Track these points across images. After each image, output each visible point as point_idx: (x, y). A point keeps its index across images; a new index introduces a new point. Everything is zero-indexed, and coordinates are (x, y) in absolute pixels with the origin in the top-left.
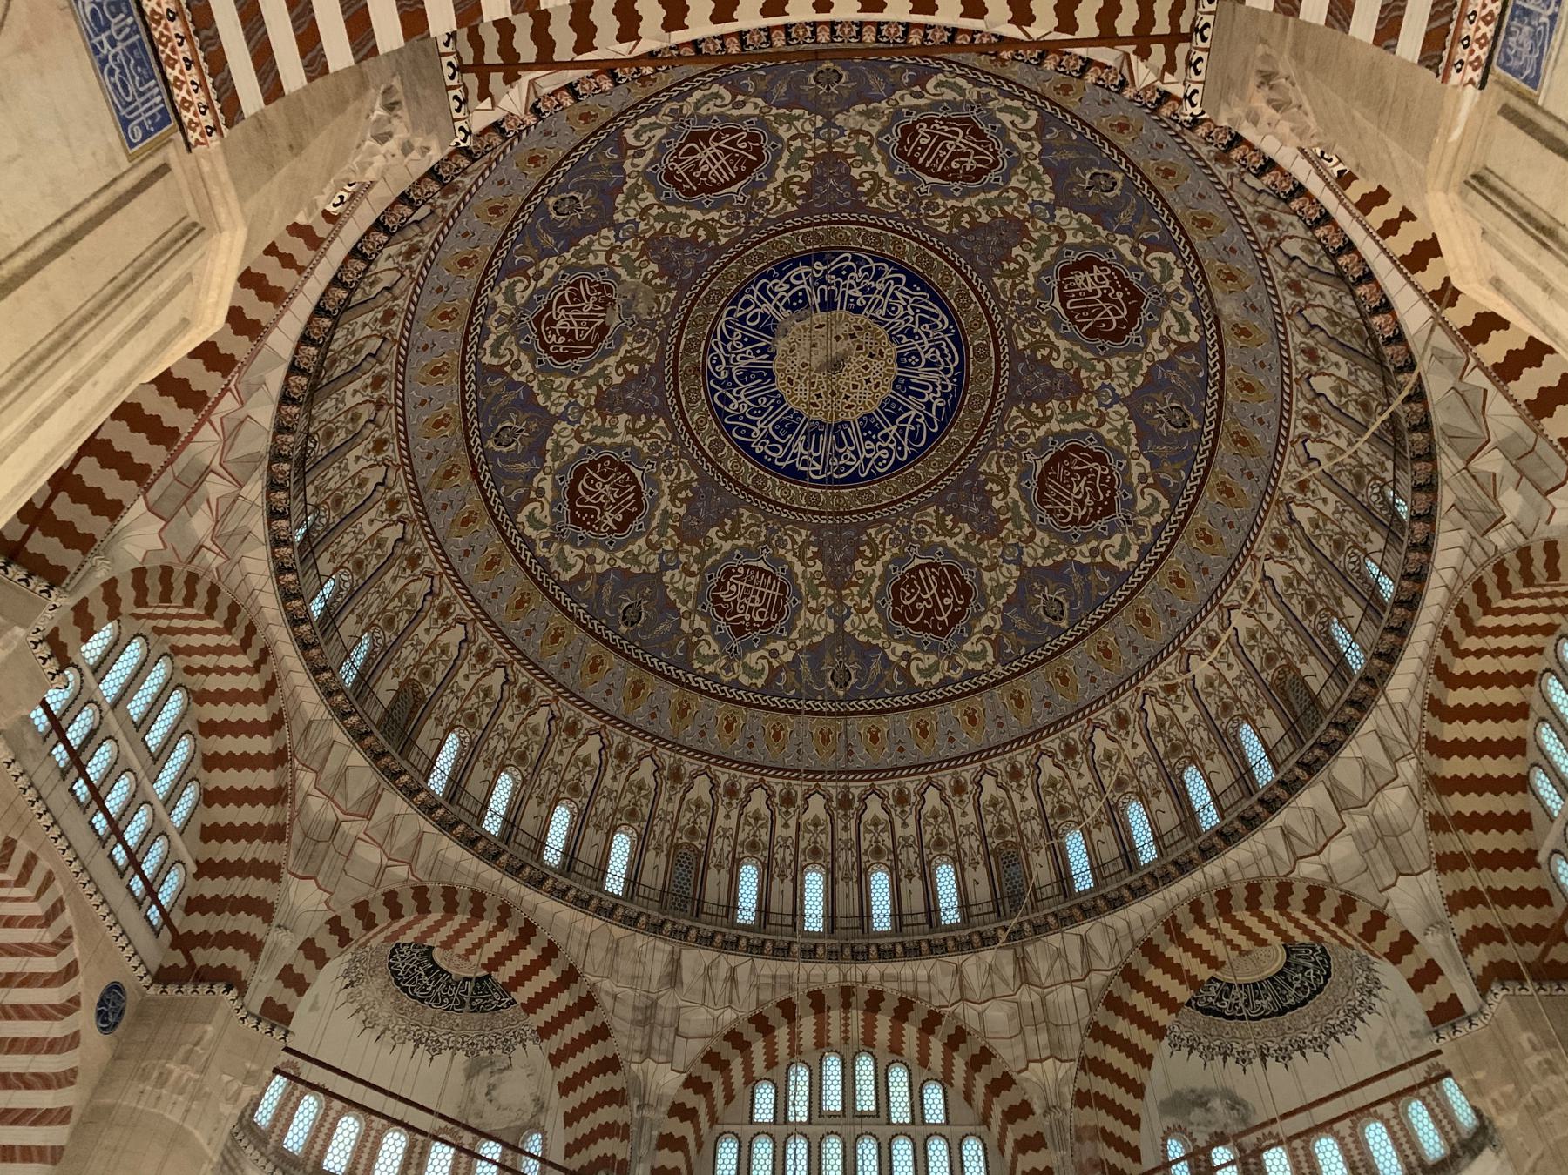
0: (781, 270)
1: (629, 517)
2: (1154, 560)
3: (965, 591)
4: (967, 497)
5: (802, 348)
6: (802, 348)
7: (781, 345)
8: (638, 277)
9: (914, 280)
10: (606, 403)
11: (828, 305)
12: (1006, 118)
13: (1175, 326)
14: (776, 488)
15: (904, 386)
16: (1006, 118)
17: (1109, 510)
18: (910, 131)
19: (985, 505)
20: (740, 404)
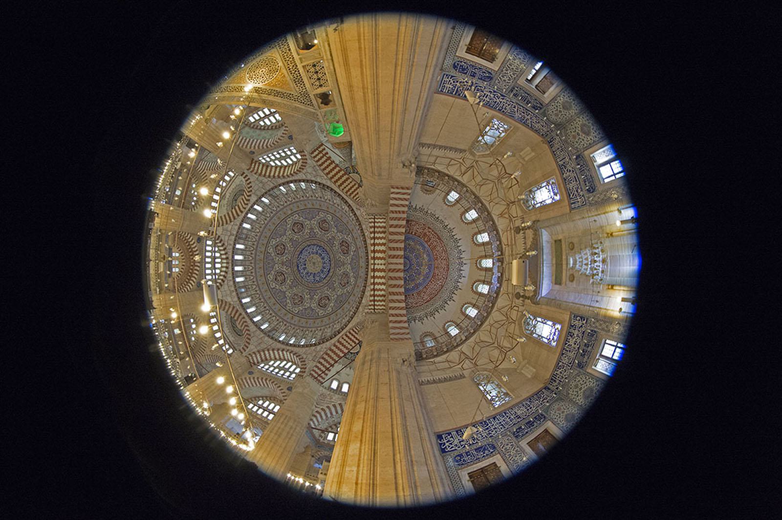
0: (299, 271)
1: (328, 299)
2: (328, 212)
3: (343, 241)
4: (331, 242)
5: (310, 268)
6: (310, 268)
7: (310, 271)
8: (295, 290)
9: (301, 252)
10: (311, 298)
11: (305, 265)
12: (274, 243)
13: (296, 217)
14: (331, 274)
15: (317, 253)
16: (274, 243)
17: (325, 220)
18: (278, 254)
19: (331, 239)
20: (318, 279)
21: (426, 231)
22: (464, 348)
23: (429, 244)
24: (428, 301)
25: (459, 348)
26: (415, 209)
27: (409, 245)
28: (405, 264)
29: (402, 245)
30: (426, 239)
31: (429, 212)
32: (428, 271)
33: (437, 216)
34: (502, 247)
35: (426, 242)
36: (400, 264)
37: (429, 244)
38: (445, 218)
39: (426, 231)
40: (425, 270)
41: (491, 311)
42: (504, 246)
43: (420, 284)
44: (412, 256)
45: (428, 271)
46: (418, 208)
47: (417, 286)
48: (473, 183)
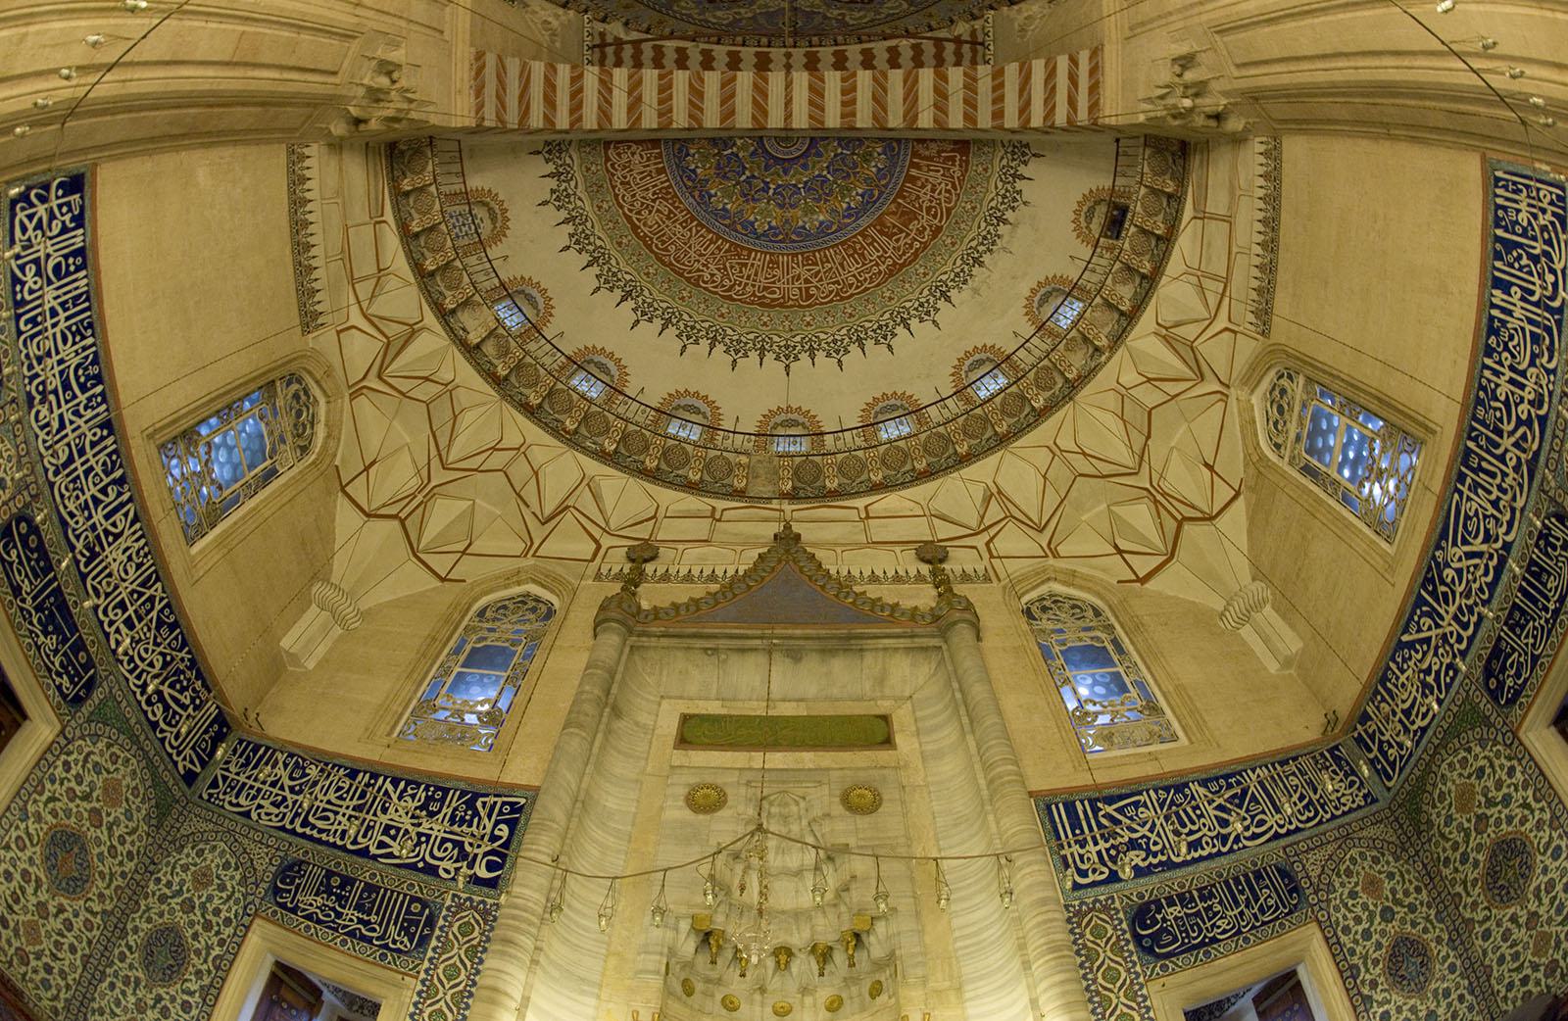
21: (925, 219)
22: (432, 341)
23: (871, 232)
24: (635, 228)
25: (430, 320)
26: (1014, 176)
27: (867, 158)
28: (786, 136)
29: (863, 120)
30: (890, 220)
31: (1002, 229)
32: (761, 227)
33: (986, 258)
34: (858, 494)
35: (880, 221)
36: (788, 116)
37: (871, 232)
38: (976, 291)
39: (925, 219)
40: (765, 215)
41: (585, 451)
42: (860, 503)
43: (704, 199)
44: (819, 167)
45: (761, 227)
46: (1019, 185)
47: (698, 188)
48: (1130, 378)
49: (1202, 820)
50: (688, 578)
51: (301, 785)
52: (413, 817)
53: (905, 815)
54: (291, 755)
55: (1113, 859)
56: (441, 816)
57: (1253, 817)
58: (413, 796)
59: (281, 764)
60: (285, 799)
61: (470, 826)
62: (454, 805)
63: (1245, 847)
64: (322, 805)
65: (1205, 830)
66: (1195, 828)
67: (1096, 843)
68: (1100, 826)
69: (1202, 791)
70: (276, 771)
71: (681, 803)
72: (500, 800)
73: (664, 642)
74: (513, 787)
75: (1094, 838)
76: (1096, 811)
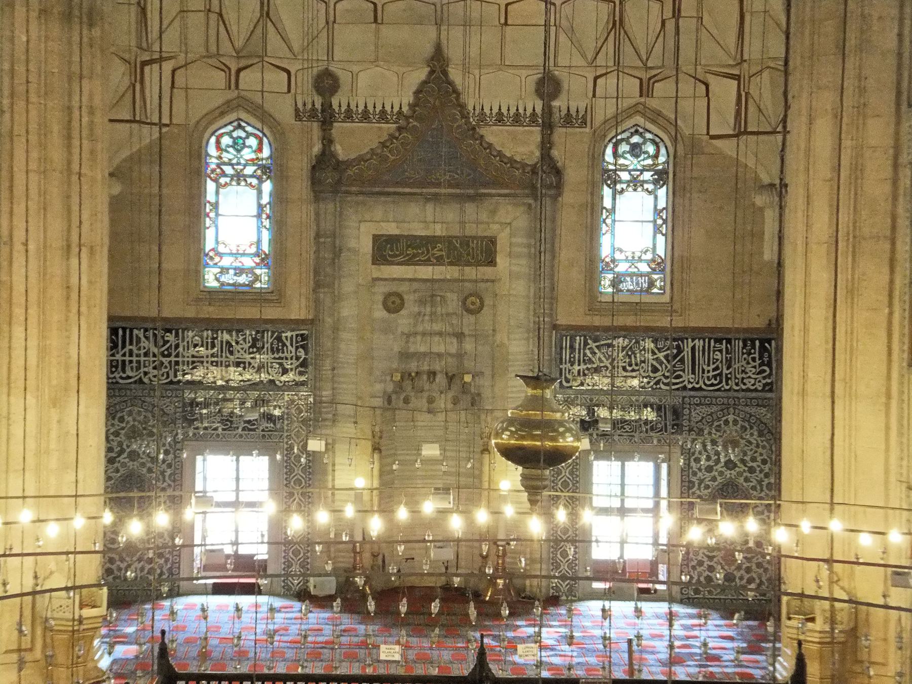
49: (643, 365)
50: (365, 116)
51: (167, 350)
52: (250, 353)
53: (495, 315)
54: (146, 330)
55: (585, 375)
56: (265, 349)
57: (675, 371)
58: (244, 340)
59: (143, 339)
60: (162, 363)
61: (283, 352)
62: (270, 341)
63: (660, 388)
64: (190, 359)
65: (642, 371)
66: (637, 368)
67: (579, 365)
68: (585, 355)
69: (652, 345)
70: (142, 344)
71: (381, 307)
72: (294, 333)
73: (361, 198)
74: (298, 323)
75: (579, 361)
76: (586, 344)
